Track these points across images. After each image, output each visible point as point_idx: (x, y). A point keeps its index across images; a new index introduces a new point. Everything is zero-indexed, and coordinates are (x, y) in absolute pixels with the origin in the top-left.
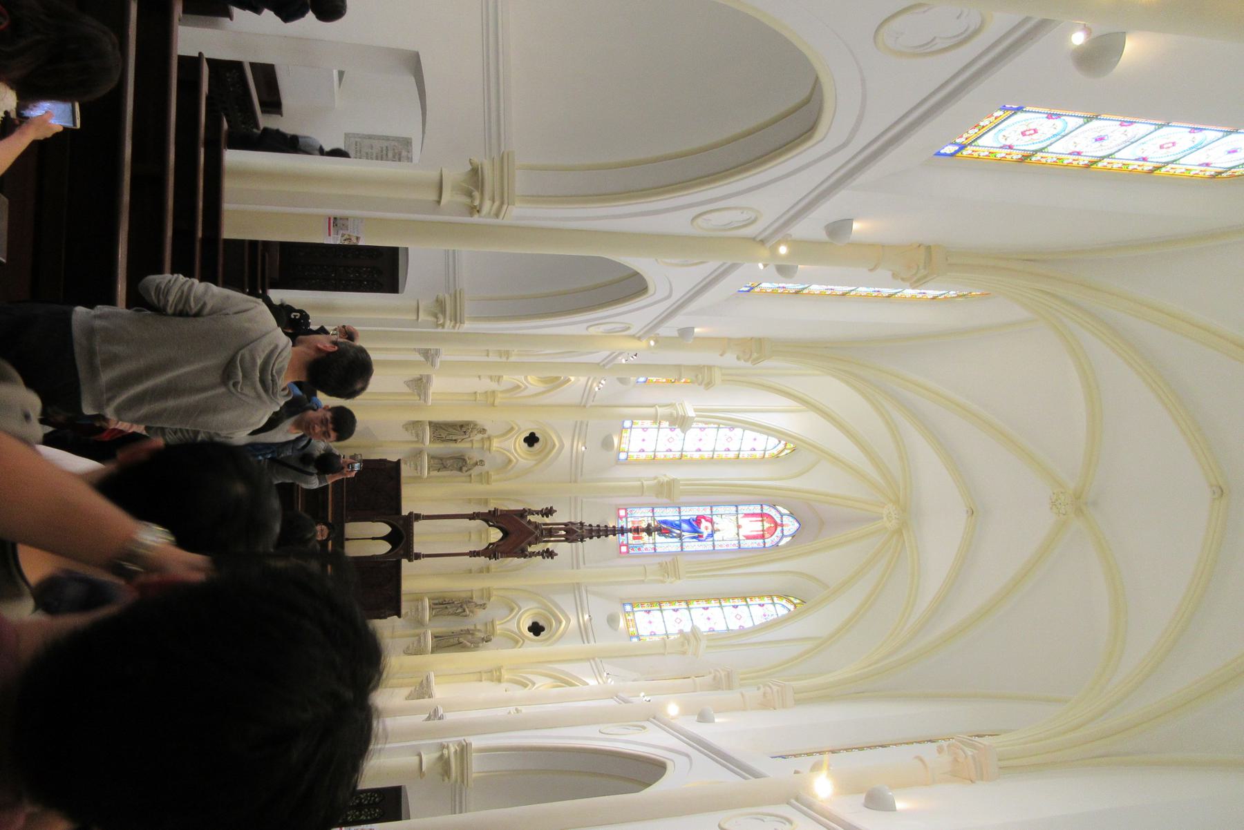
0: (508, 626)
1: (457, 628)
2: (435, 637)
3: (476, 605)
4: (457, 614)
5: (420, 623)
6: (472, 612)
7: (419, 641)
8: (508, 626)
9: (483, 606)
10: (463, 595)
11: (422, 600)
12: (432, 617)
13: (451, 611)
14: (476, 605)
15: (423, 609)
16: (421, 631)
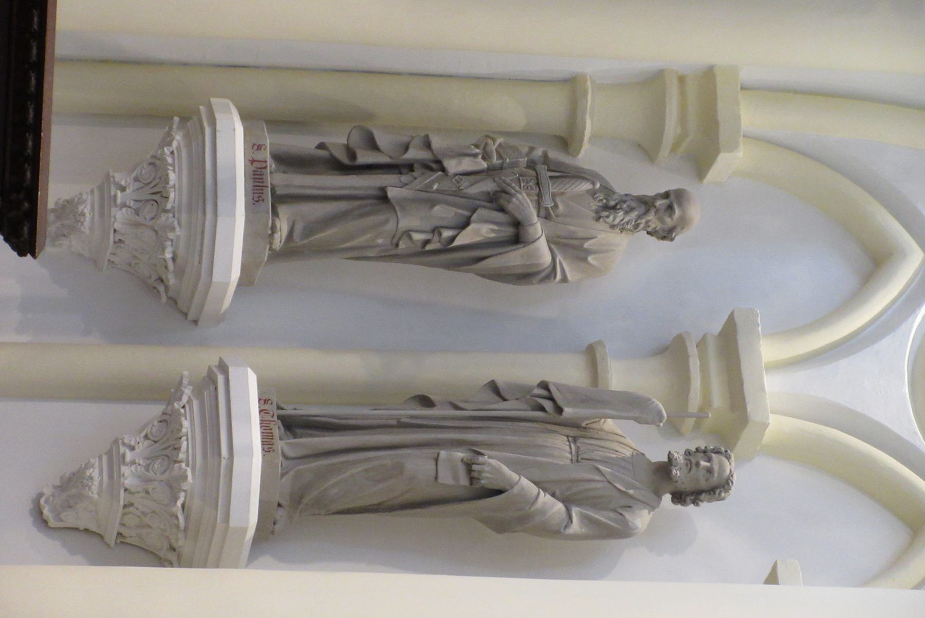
0: (842, 384)
1: (460, 369)
2: (289, 423)
3: (609, 204)
4: (469, 259)
5: (165, 295)
6: (572, 247)
7: (165, 443)
8: (842, 384)
9: (662, 214)
10: (509, 111)
11: (193, 120)
12: (275, 256)
13: (414, 223)
14: (609, 204)
15: (204, 194)
16: (184, 360)
